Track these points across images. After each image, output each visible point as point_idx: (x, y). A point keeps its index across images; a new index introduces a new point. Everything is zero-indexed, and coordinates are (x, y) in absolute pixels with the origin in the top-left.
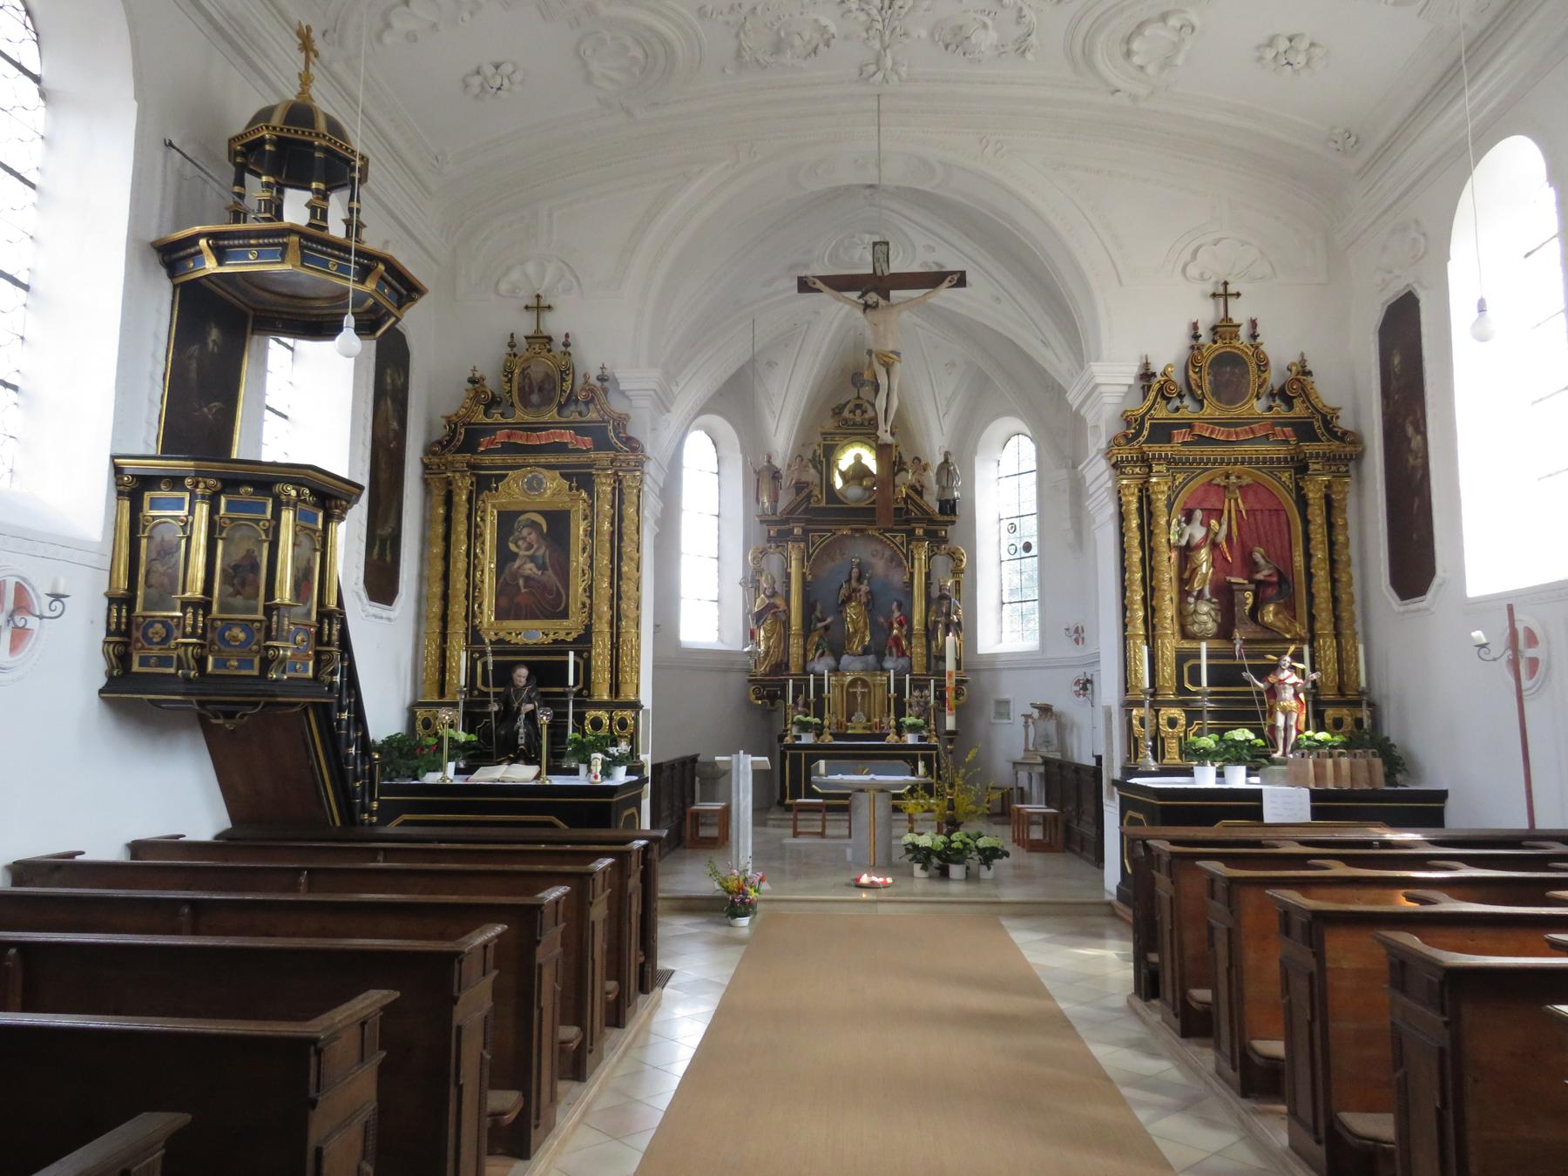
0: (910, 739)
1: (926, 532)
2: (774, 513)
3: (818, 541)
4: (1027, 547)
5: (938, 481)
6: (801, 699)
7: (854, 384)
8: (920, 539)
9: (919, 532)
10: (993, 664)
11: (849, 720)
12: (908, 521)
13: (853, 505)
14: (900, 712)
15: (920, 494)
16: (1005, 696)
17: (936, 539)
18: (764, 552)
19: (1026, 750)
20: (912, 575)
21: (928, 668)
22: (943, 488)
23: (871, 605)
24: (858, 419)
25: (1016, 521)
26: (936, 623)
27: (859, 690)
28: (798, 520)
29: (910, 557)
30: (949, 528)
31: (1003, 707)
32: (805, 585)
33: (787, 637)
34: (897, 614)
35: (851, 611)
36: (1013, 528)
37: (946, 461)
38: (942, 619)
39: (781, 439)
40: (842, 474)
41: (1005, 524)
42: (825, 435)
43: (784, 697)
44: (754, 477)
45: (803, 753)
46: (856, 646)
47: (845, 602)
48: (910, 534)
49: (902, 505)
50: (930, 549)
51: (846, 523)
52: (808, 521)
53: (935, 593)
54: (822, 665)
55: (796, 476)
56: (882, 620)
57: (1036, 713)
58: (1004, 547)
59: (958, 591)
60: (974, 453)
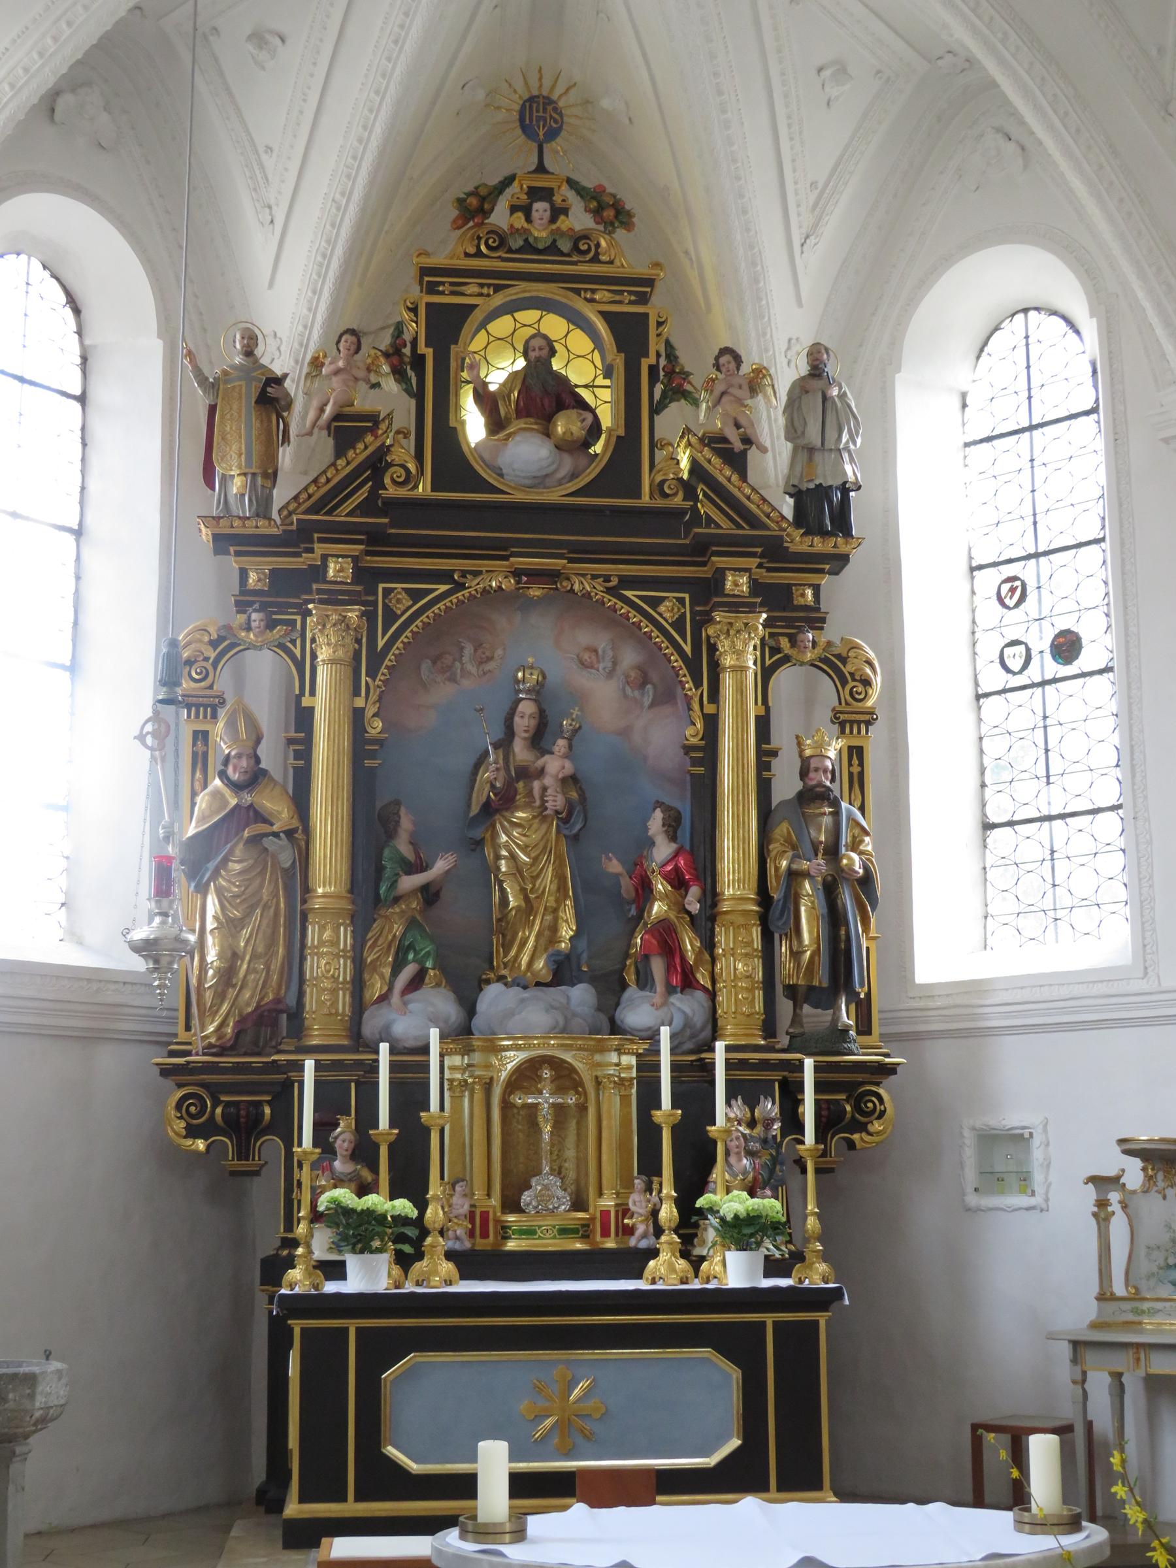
0: (736, 1270)
1: (756, 587)
2: (263, 508)
3: (402, 604)
4: (1066, 647)
5: (793, 432)
6: (344, 1133)
7: (526, 129)
8: (735, 606)
9: (737, 584)
10: (968, 1019)
11: (512, 1204)
12: (701, 550)
13: (519, 497)
14: (694, 1177)
15: (737, 461)
16: (1012, 1118)
17: (790, 618)
18: (225, 644)
19: (1105, 1296)
20: (712, 724)
21: (769, 1028)
22: (806, 453)
23: (576, 820)
24: (540, 233)
25: (1027, 572)
26: (794, 876)
27: (545, 1099)
28: (338, 533)
29: (705, 666)
30: (825, 581)
31: (1005, 1157)
32: (362, 749)
33: (298, 919)
34: (663, 850)
35: (514, 839)
36: (1015, 593)
37: (817, 371)
38: (818, 865)
39: (292, 293)
40: (484, 398)
41: (989, 581)
42: (431, 277)
43: (286, 1128)
44: (201, 400)
45: (352, 1326)
46: (529, 955)
47: (489, 811)
48: (707, 592)
49: (678, 501)
50: (769, 647)
51: (499, 550)
52: (376, 540)
53: (786, 786)
54: (420, 1019)
55: (333, 392)
56: (614, 866)
57: (1134, 1173)
58: (989, 647)
59: (858, 781)
60: (891, 363)
